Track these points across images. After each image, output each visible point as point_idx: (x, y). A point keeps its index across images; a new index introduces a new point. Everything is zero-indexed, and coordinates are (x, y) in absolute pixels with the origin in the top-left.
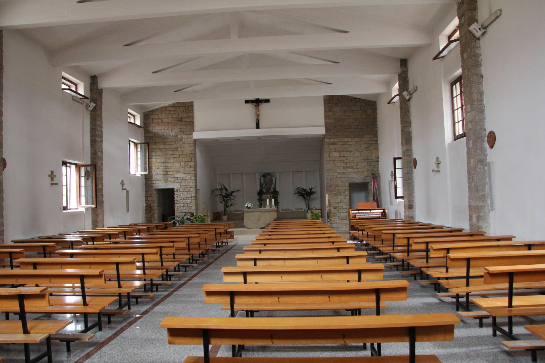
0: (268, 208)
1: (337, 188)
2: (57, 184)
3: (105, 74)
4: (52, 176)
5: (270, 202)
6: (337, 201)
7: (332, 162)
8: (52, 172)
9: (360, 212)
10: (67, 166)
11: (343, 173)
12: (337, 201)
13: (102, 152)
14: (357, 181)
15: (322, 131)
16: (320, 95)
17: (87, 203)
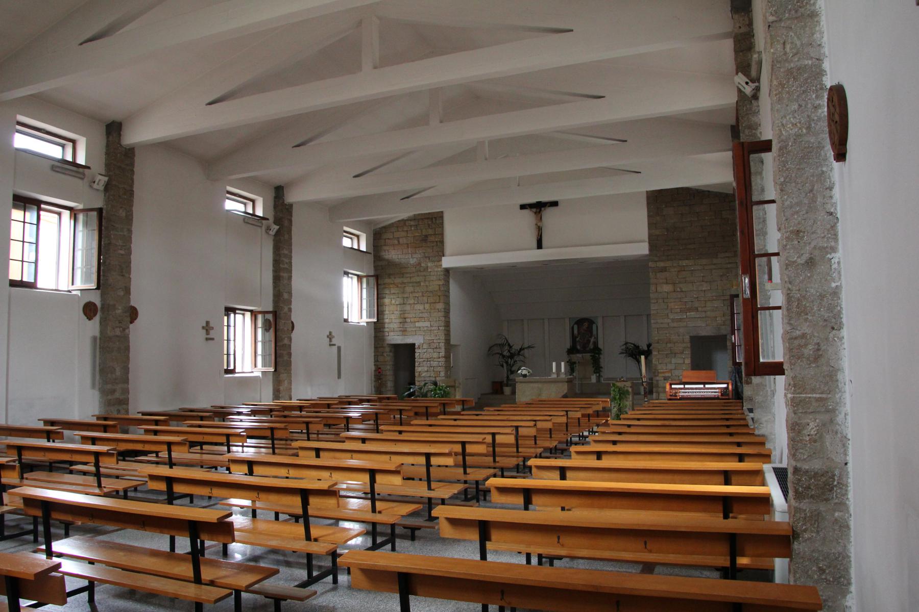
0: (554, 376)
1: (669, 345)
2: (212, 339)
3: (292, 183)
4: (207, 328)
5: (559, 367)
6: (670, 367)
7: (660, 301)
8: (208, 323)
9: (687, 386)
10: (235, 313)
11: (681, 320)
12: (670, 367)
13: (290, 293)
14: (703, 333)
15: (643, 249)
16: (640, 190)
17: (264, 365)
